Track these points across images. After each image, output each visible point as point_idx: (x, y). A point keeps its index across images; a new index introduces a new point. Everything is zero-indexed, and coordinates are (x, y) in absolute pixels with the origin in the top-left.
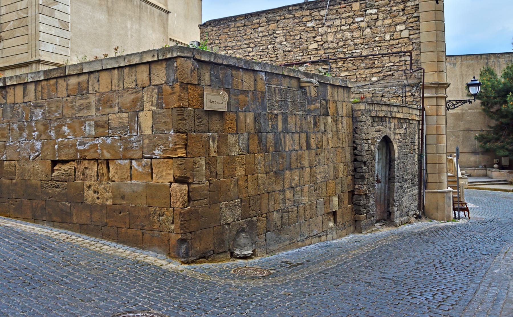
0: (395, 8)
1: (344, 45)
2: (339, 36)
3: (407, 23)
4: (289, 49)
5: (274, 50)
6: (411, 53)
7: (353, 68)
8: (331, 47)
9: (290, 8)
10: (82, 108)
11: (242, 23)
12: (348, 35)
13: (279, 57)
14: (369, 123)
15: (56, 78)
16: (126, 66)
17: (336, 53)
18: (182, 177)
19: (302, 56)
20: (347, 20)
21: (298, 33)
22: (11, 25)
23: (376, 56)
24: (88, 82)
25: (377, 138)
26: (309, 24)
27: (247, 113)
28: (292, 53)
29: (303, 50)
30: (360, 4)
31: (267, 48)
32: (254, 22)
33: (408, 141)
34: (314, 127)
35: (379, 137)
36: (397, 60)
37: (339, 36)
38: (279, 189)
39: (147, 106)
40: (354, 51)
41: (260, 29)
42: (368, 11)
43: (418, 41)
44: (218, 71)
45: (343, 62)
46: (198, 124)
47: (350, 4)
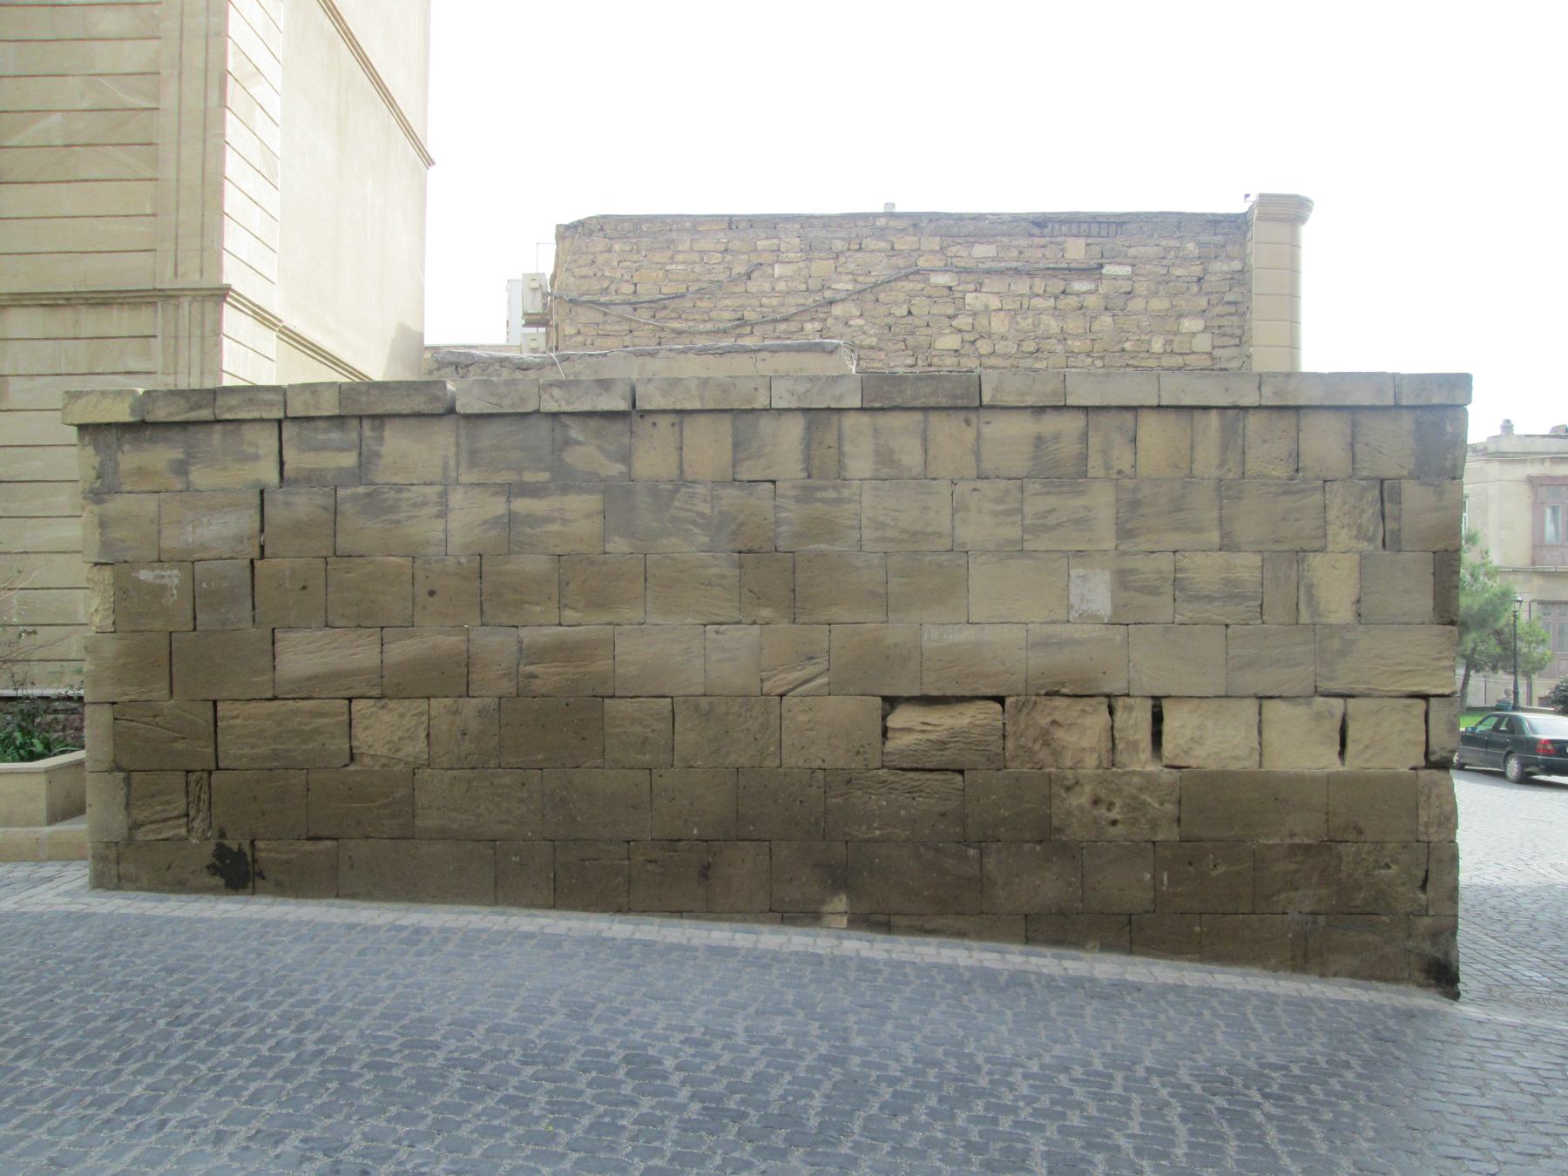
0: (1179, 272)
4: (874, 341)
9: (881, 222)
10: (1051, 520)
11: (718, 241)
12: (1053, 325)
15: (925, 409)
21: (902, 297)
24: (1085, 437)
28: (882, 355)
29: (915, 351)
31: (802, 329)
32: (761, 244)
37: (1025, 324)
39: (1341, 537)
47: (1061, 239)
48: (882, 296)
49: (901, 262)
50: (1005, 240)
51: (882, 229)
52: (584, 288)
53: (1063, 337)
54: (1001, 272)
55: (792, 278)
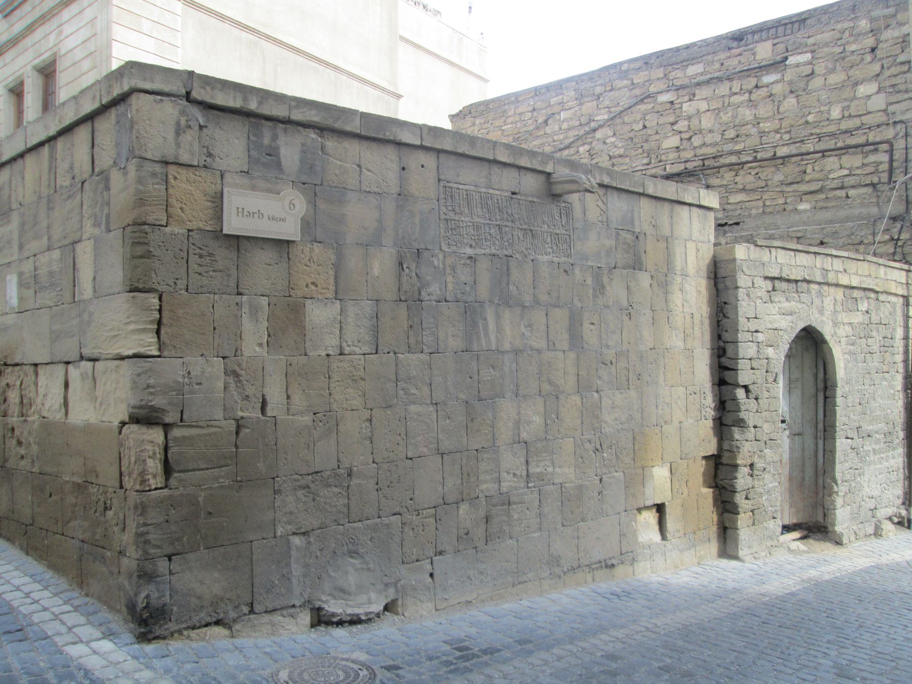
0: (853, 47)
1: (738, 136)
2: (725, 117)
3: (880, 78)
4: (621, 151)
6: (892, 145)
7: (756, 185)
9: (625, 67)
12: (747, 114)
14: (762, 293)
18: (141, 407)
19: (648, 164)
20: (744, 82)
21: (638, 116)
23: (808, 157)
25: (786, 331)
30: (774, 45)
31: (578, 152)
33: (875, 344)
34: (595, 296)
35: (790, 328)
36: (858, 163)
37: (725, 117)
41: (563, 115)
42: (790, 59)
44: (275, 138)
45: (733, 173)
46: (200, 269)
47: (750, 47)
48: (626, 119)
49: (637, 92)
50: (710, 57)
51: (626, 72)
53: (757, 121)
54: (708, 82)
55: (571, 119)
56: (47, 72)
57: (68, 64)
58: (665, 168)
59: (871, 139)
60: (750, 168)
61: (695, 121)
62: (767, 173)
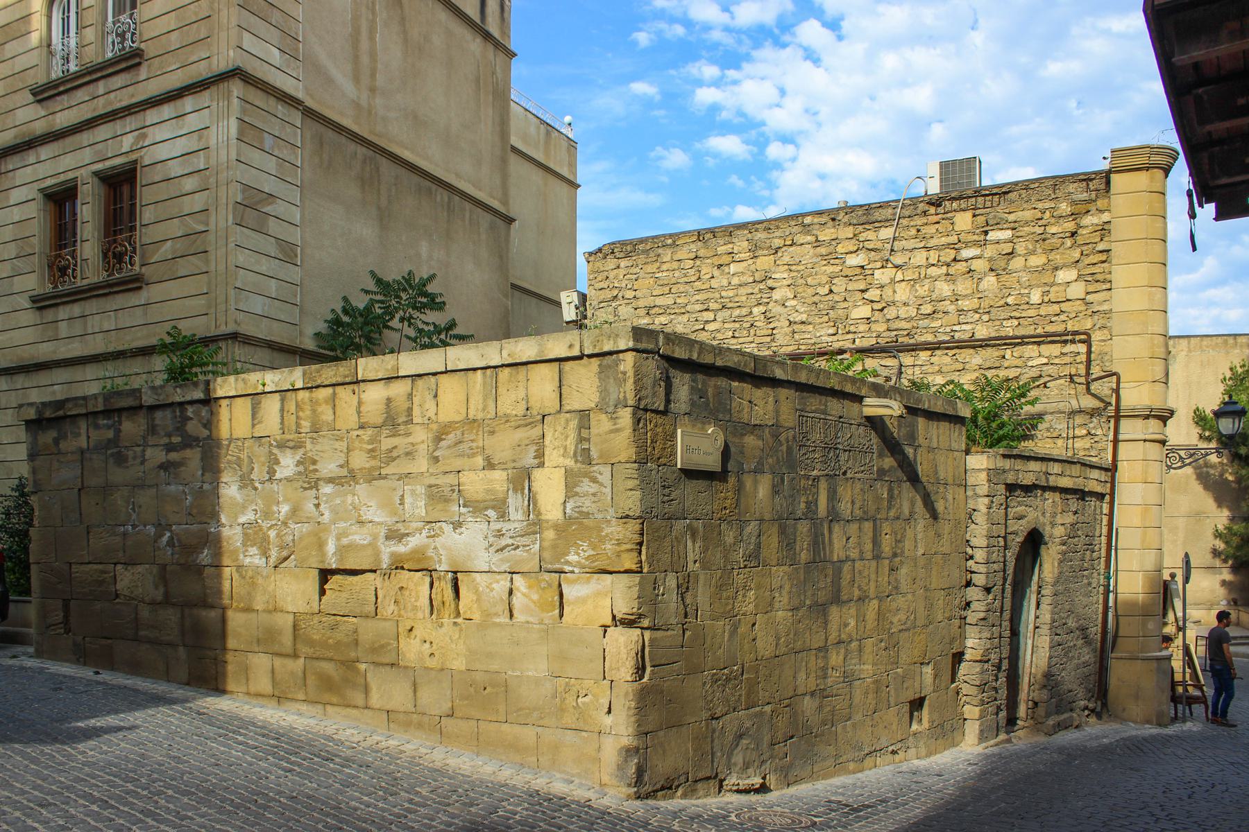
0: (1053, 230)
2: (922, 290)
3: (1080, 265)
4: (804, 317)
5: (768, 320)
7: (953, 367)
8: (903, 316)
9: (808, 220)
10: (395, 454)
11: (690, 251)
12: (944, 289)
13: (777, 337)
16: (503, 366)
17: (914, 331)
20: (942, 253)
21: (824, 279)
22: (166, 249)
24: (410, 396)
26: (853, 260)
27: (759, 476)
28: (810, 328)
32: (721, 250)
37: (922, 290)
38: (816, 646)
39: (553, 457)
40: (957, 328)
41: (733, 268)
42: (991, 234)
43: (1105, 307)
47: (949, 215)
52: (601, 298)
53: (956, 299)
56: (121, 184)
57: (157, 179)
58: (854, 341)
59: (1070, 328)
60: (948, 348)
61: (888, 292)
62: (965, 355)
